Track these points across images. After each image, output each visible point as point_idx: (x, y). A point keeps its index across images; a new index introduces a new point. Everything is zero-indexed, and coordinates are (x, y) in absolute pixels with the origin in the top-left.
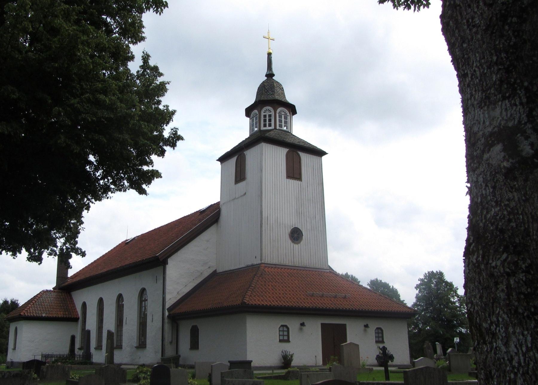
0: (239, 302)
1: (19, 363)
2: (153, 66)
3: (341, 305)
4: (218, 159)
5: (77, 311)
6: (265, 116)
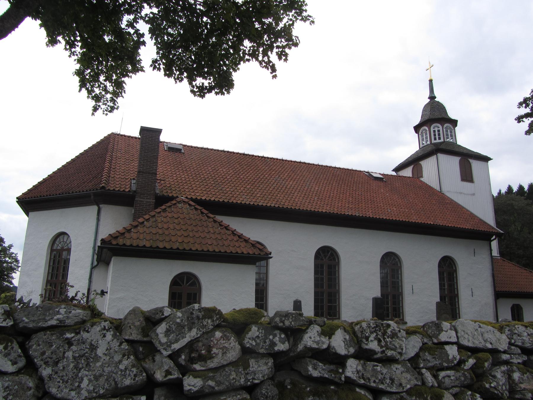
6: (434, 131)
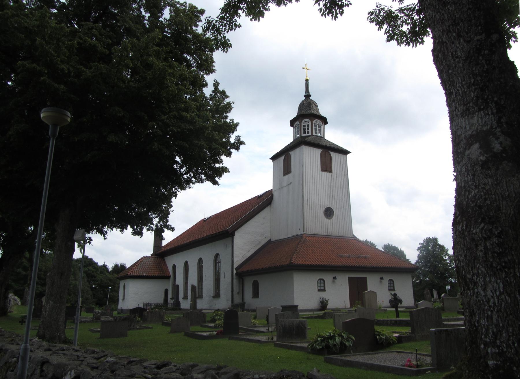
0: (288, 263)
1: (127, 310)
2: (221, 90)
3: (363, 263)
4: (270, 158)
5: (169, 271)
6: (304, 126)
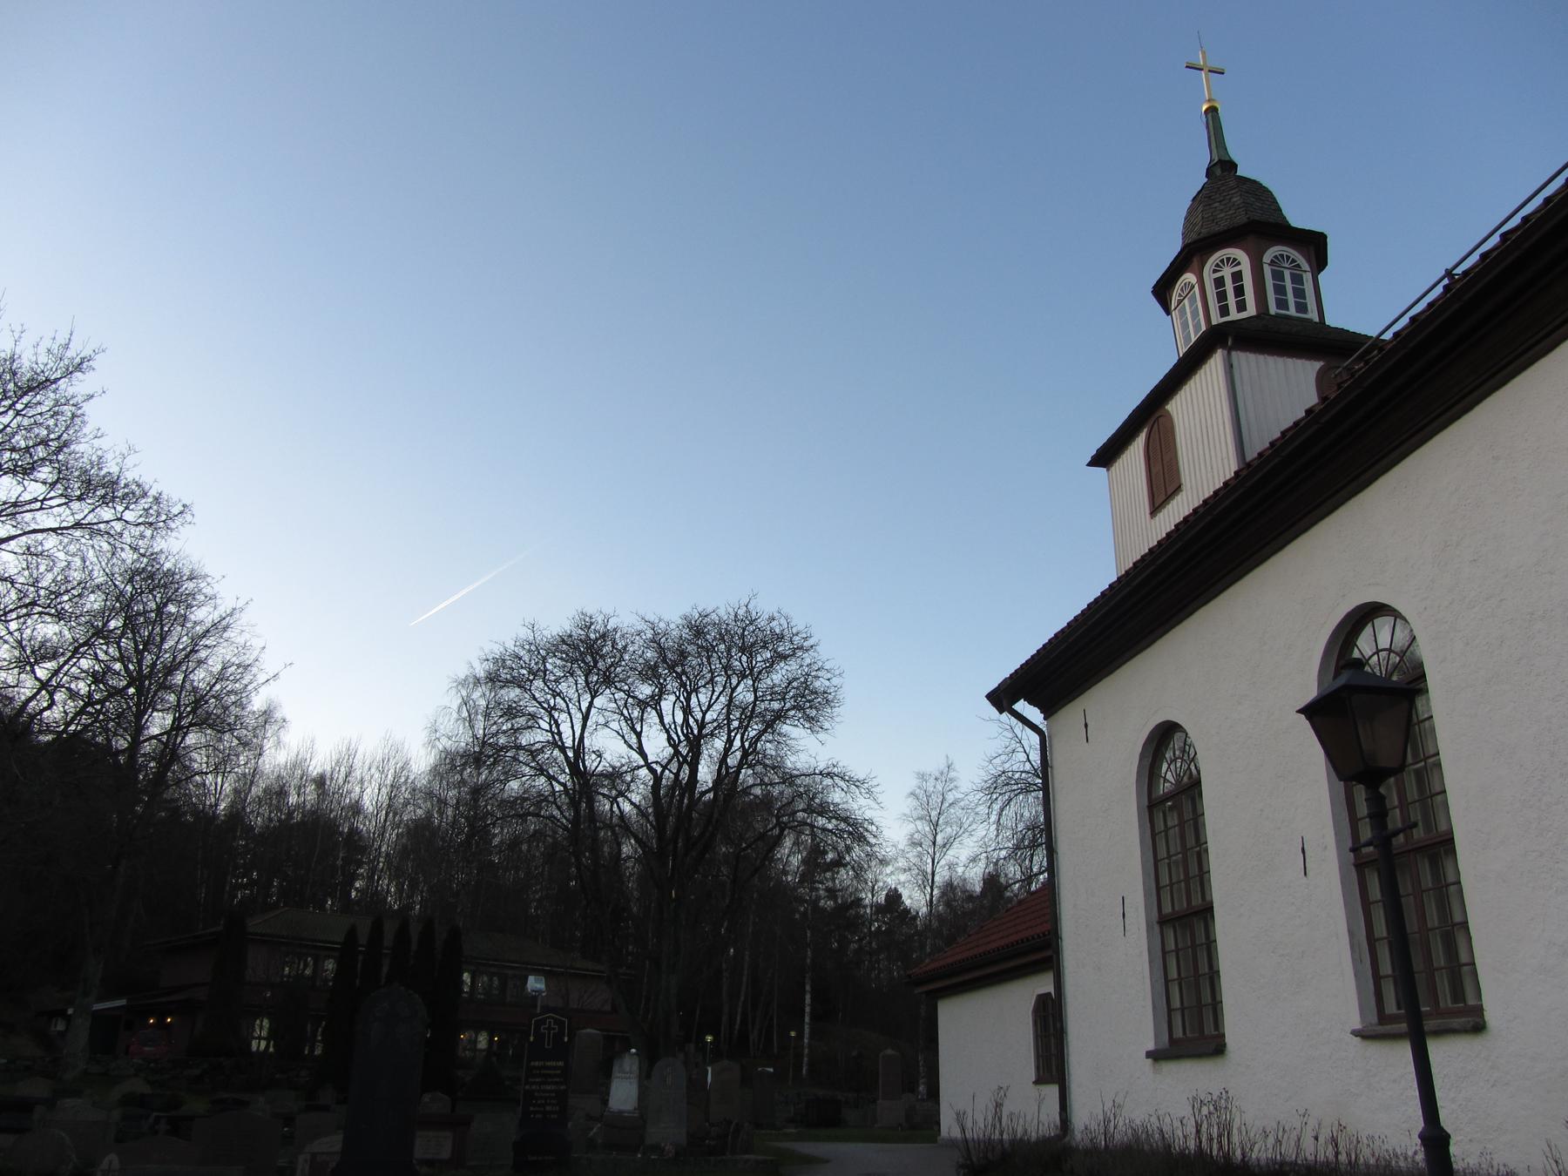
6: (1219, 282)
